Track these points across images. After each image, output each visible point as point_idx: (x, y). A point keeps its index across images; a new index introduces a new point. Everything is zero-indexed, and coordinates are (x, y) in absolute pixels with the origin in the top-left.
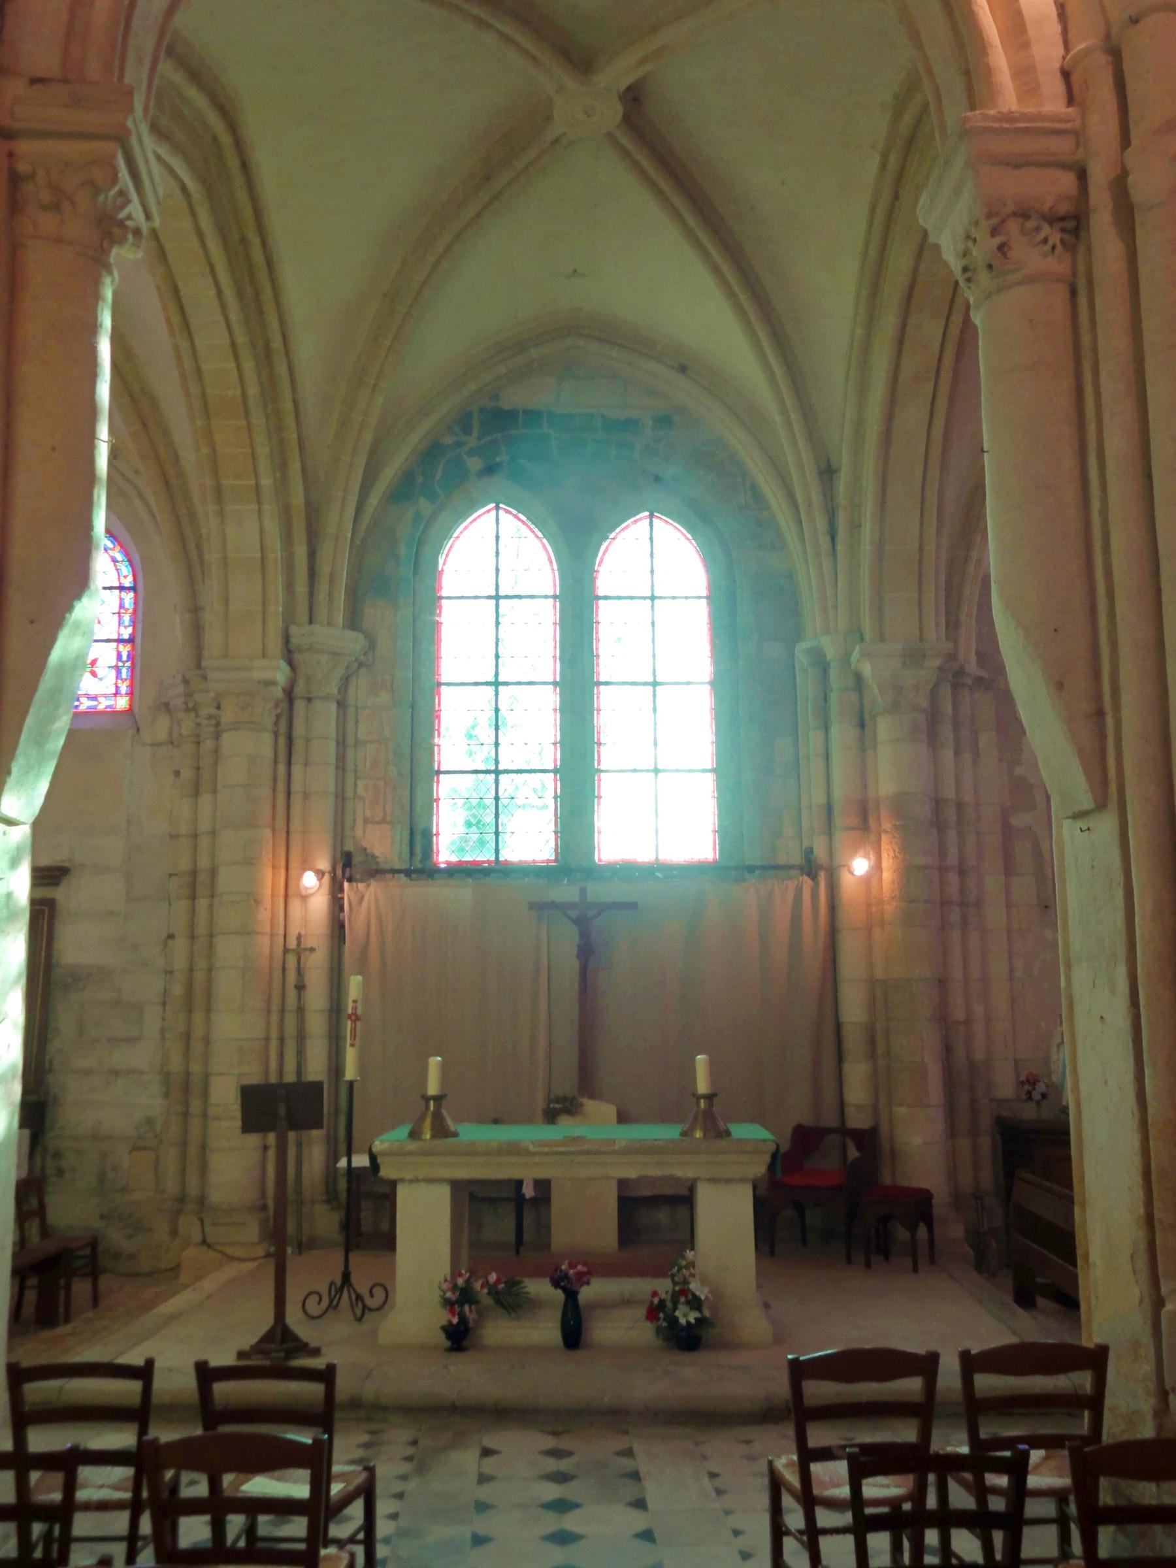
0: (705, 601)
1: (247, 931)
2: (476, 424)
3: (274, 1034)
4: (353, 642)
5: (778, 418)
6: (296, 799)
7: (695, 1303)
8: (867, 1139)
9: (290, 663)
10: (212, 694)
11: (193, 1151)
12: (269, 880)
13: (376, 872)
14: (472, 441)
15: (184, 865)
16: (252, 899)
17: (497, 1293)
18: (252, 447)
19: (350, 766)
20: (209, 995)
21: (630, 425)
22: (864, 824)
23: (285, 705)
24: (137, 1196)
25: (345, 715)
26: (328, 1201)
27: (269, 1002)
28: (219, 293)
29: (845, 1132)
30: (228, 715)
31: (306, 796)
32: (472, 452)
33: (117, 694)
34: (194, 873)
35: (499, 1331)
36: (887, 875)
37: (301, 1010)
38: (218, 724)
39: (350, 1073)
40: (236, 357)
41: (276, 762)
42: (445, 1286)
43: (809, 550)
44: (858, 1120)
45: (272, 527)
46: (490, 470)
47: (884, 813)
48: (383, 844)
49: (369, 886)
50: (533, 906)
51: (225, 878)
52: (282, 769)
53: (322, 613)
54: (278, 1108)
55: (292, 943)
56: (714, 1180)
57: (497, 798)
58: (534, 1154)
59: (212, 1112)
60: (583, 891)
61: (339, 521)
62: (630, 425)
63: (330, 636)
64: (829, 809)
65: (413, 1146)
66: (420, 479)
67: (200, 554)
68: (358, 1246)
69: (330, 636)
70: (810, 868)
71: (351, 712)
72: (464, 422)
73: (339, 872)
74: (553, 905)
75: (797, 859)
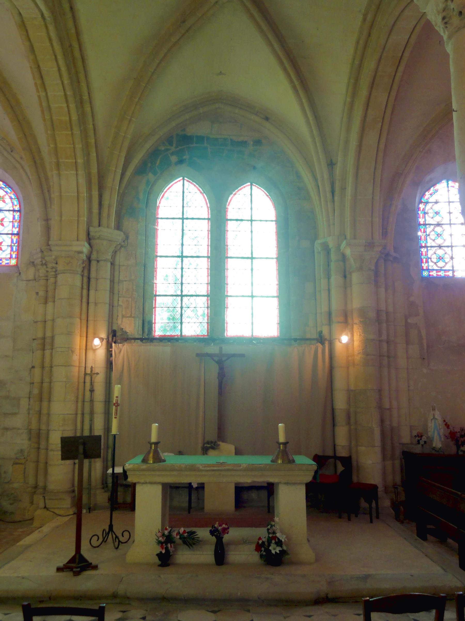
0: (274, 222)
1: (68, 365)
3: (80, 412)
4: (118, 236)
5: (310, 140)
6: (92, 306)
7: (279, 543)
8: (347, 461)
9: (90, 244)
10: (54, 257)
11: (41, 465)
12: (78, 342)
13: (126, 339)
14: (173, 149)
15: (40, 335)
16: (70, 350)
17: (185, 538)
18: (74, 143)
19: (116, 291)
20: (50, 393)
21: (244, 143)
22: (346, 321)
23: (87, 263)
24: (15, 485)
25: (114, 269)
26: (103, 488)
27: (77, 397)
28: (59, 70)
29: (335, 457)
30: (60, 267)
31: (96, 304)
32: (172, 154)
33: (11, 258)
34: (44, 338)
35: (184, 556)
36: (357, 343)
37: (92, 401)
38: (56, 271)
39: (114, 431)
40: (67, 101)
41: (82, 288)
42: (159, 534)
43: (322, 200)
44: (342, 453)
45: (82, 181)
46: (181, 162)
47: (355, 315)
48: (130, 326)
49: (123, 345)
50: (198, 355)
51: (59, 341)
52: (85, 292)
53: (104, 221)
54: (79, 448)
55: (88, 371)
56: (287, 484)
58: (202, 470)
59: (50, 447)
60: (221, 349)
61: (113, 181)
62: (244, 143)
63: (108, 232)
64: (330, 314)
65: (144, 466)
66: (149, 165)
67: (50, 194)
68: (116, 509)
69: (108, 232)
70: (321, 340)
71: (117, 267)
72: (169, 140)
73: (110, 339)
74: (208, 355)
75: (315, 336)
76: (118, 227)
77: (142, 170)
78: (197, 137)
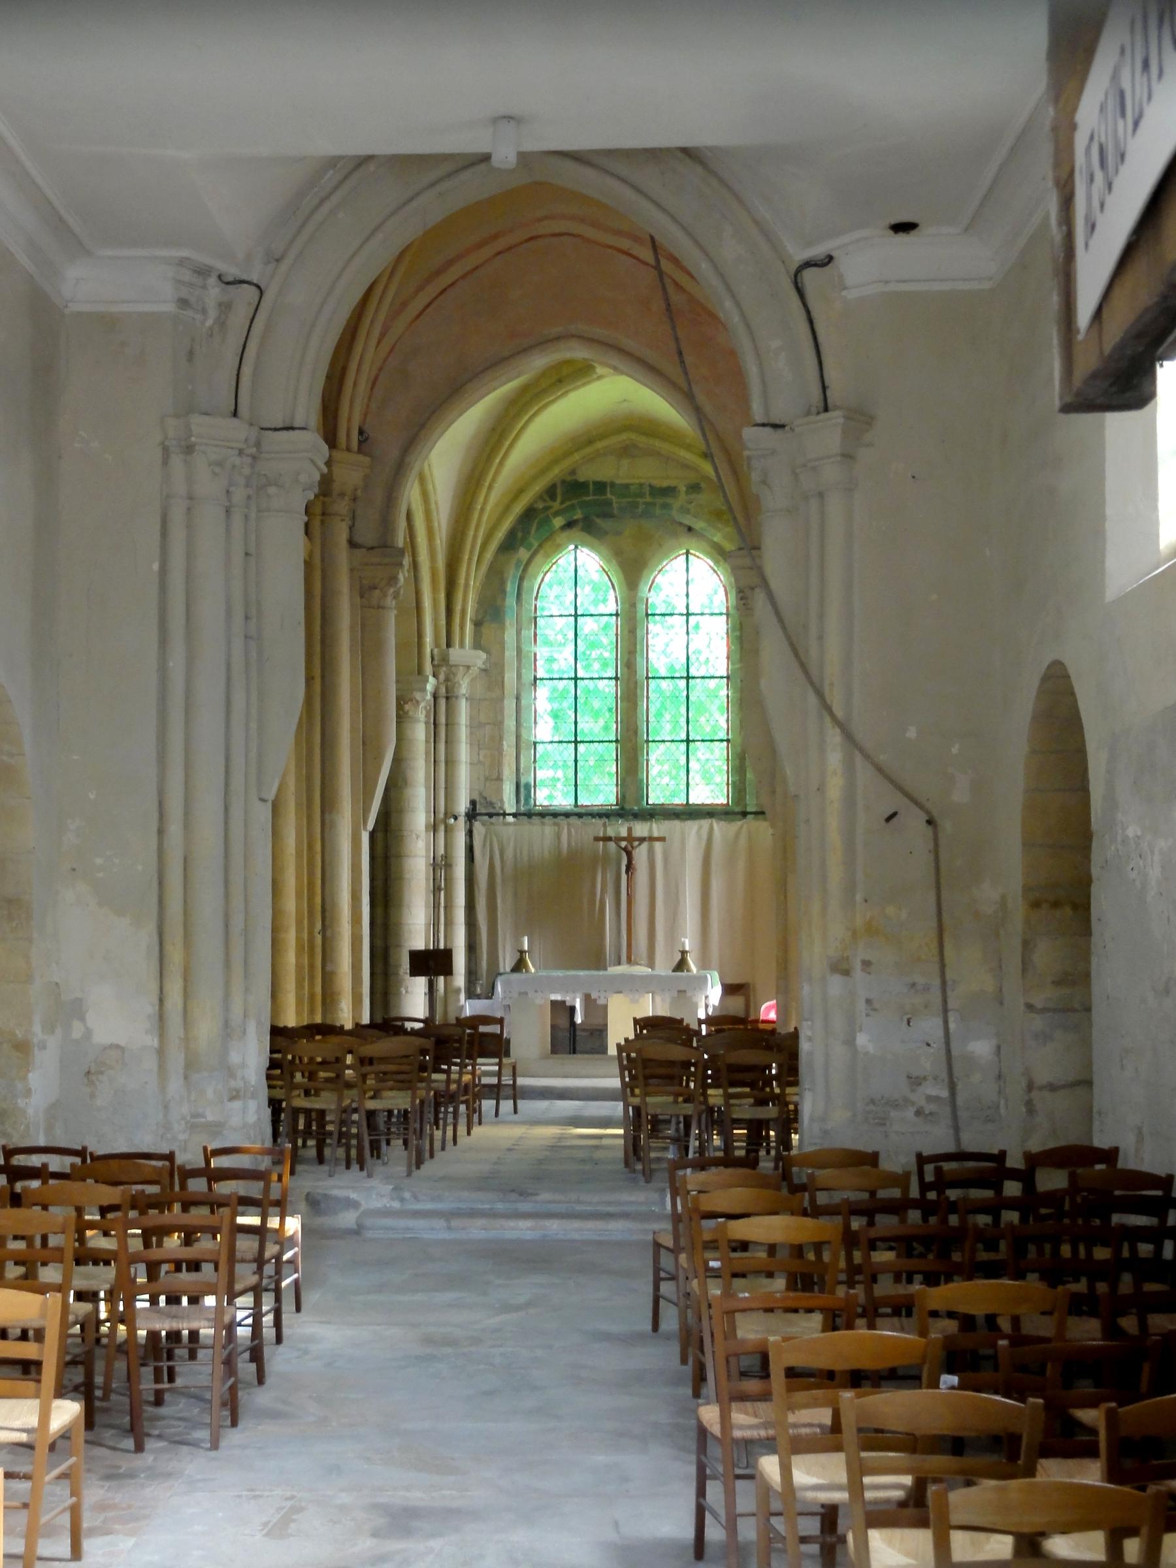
0: (725, 617)
2: (559, 491)
14: (556, 505)
32: (556, 514)
57: (576, 761)
66: (520, 535)
72: (551, 492)
76: (477, 645)
77: (510, 544)
78: (596, 483)
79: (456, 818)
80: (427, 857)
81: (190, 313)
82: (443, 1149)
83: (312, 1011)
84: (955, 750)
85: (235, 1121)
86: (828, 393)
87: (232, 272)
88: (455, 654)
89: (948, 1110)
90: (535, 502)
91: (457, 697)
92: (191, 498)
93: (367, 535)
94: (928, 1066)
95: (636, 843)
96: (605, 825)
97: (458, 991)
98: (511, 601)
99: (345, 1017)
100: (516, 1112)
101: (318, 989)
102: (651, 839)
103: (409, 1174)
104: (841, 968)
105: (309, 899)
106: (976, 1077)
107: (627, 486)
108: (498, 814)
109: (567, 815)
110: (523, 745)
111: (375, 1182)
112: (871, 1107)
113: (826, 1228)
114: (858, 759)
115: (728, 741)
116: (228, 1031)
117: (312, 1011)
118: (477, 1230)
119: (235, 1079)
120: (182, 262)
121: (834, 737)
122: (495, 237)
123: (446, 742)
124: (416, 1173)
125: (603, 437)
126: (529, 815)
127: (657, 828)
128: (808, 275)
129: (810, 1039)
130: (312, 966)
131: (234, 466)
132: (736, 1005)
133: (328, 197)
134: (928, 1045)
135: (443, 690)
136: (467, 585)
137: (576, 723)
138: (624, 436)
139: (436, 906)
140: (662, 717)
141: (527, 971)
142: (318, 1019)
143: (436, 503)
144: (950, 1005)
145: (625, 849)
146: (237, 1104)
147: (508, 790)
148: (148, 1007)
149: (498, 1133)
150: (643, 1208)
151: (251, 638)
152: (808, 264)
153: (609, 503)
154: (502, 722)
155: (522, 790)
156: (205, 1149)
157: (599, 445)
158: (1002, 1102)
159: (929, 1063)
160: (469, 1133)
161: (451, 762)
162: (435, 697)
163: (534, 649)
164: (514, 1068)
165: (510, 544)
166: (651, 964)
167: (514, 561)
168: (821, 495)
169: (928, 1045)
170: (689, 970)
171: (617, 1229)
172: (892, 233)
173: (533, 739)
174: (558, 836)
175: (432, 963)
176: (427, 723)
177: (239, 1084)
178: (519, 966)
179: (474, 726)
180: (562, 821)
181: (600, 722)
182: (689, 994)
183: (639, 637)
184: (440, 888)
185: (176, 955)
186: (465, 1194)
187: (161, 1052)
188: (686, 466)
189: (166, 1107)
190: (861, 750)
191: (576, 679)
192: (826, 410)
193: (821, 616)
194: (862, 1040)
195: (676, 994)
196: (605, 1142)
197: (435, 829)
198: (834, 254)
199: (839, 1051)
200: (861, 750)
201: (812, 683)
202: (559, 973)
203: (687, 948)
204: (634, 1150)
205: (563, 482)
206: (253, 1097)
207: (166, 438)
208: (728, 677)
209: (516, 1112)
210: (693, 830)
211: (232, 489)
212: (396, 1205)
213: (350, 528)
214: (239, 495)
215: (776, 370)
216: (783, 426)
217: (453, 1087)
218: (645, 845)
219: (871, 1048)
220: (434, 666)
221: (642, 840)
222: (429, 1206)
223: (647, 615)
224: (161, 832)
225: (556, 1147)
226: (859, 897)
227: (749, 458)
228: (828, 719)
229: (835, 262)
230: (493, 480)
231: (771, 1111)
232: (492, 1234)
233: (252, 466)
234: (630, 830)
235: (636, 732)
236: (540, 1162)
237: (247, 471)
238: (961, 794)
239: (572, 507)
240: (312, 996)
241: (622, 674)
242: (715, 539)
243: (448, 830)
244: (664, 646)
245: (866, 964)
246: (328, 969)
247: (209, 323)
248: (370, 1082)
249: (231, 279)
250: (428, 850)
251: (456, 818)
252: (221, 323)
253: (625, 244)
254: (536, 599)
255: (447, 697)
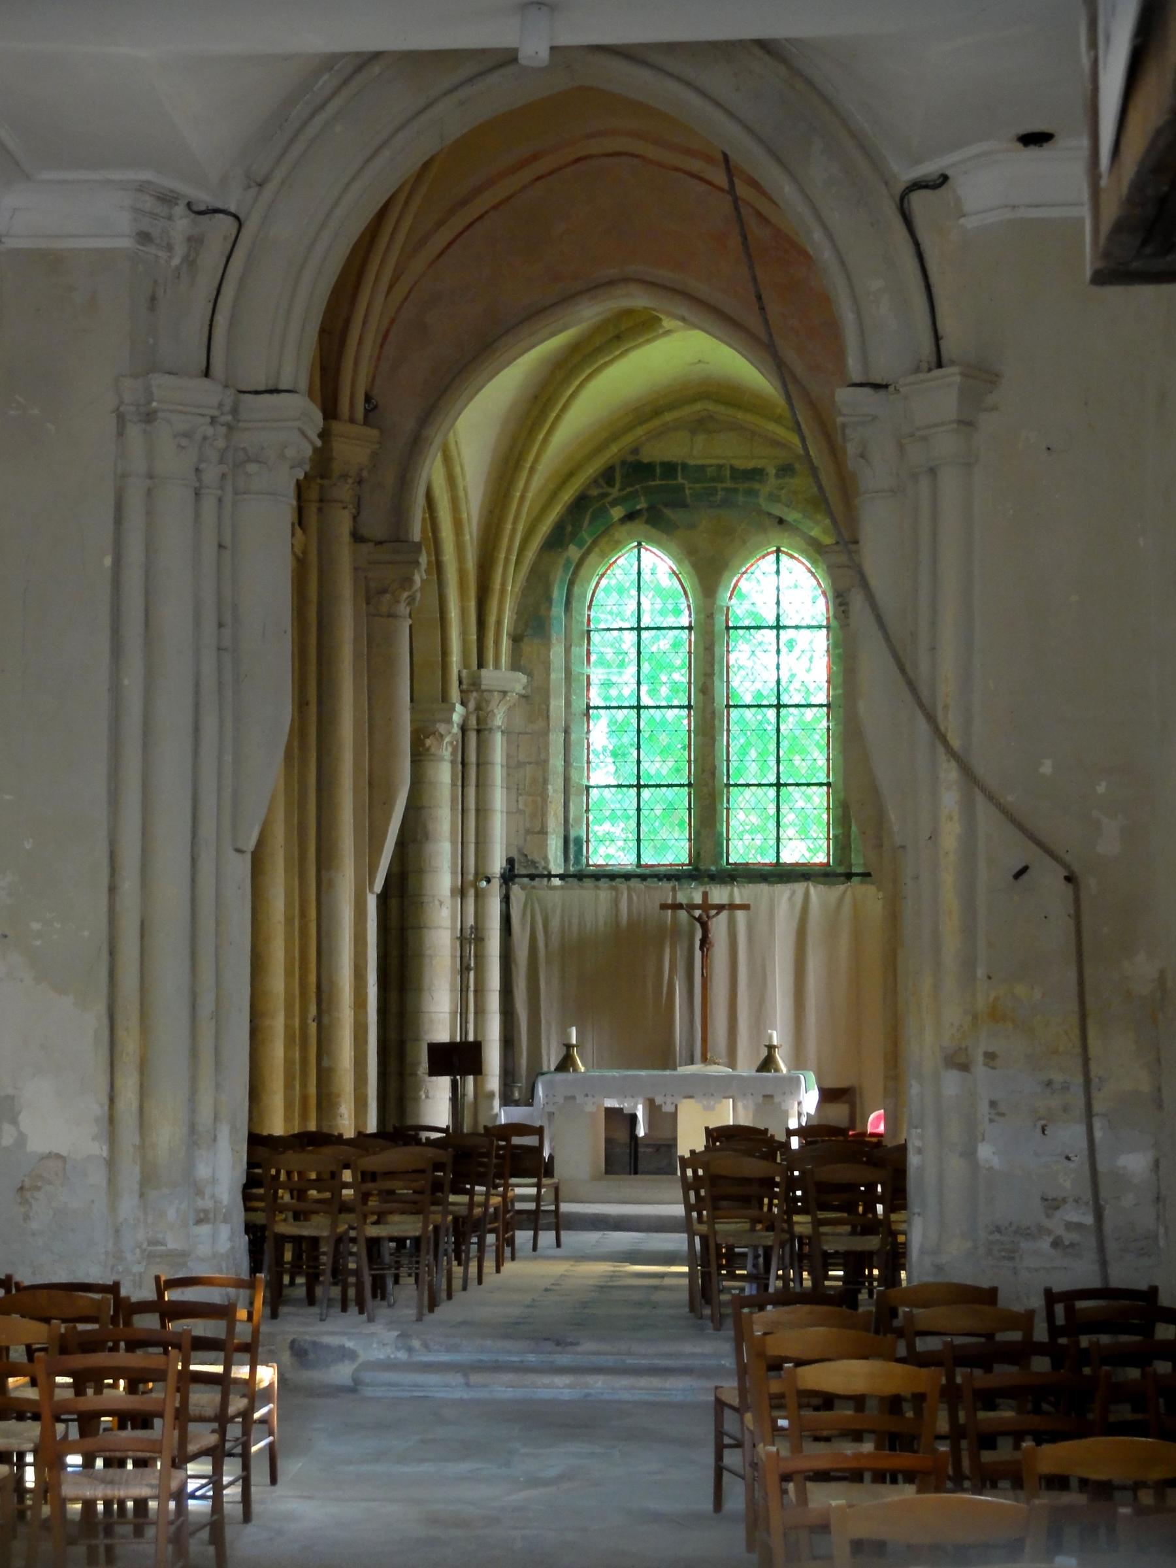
0: (824, 631)
14: (615, 492)
32: (614, 503)
57: (639, 810)
66: (569, 529)
72: (608, 475)
76: (515, 666)
79: (489, 881)
80: (453, 928)
81: (152, 249)
82: (465, 1288)
83: (304, 1116)
84: (1101, 789)
85: (203, 1250)
86: (943, 343)
87: (205, 198)
88: (489, 676)
89: (1091, 1242)
90: (588, 487)
91: (490, 730)
92: (150, 476)
93: (376, 524)
94: (1068, 1184)
95: (713, 912)
96: (674, 889)
97: (491, 1095)
98: (557, 610)
99: (346, 1125)
100: (558, 1245)
101: (312, 1090)
102: (732, 907)
103: (420, 1319)
104: (958, 1061)
105: (301, 978)
106: (1129, 1200)
107: (702, 468)
108: (542, 876)
109: (627, 876)
110: (573, 790)
111: (377, 1328)
112: (997, 1236)
113: (926, 1379)
114: (979, 797)
115: (828, 785)
116: (194, 1137)
117: (304, 1116)
118: (503, 1388)
119: (203, 1198)
120: (142, 187)
121: (950, 773)
122: (535, 157)
123: (477, 786)
124: (429, 1317)
125: (671, 407)
126: (580, 876)
127: (739, 893)
128: (918, 200)
129: (920, 1151)
130: (304, 1061)
131: (205, 438)
132: (838, 1114)
133: (322, 106)
134: (1068, 1158)
135: (473, 722)
136: (503, 591)
137: (639, 762)
138: (698, 406)
139: (464, 990)
140: (746, 753)
141: (576, 1070)
142: (312, 1127)
143: (465, 490)
144: (1097, 1107)
145: (699, 919)
146: (205, 1229)
147: (554, 845)
148: (96, 1106)
149: (536, 1270)
150: (713, 1362)
151: (225, 650)
152: (918, 185)
153: (681, 488)
154: (546, 761)
155: (572, 845)
156: (157, 1278)
157: (668, 417)
158: (1162, 1231)
159: (1069, 1181)
160: (498, 1271)
161: (482, 811)
162: (464, 729)
163: (586, 670)
164: (557, 1190)
165: (557, 540)
166: (732, 1064)
167: (562, 562)
168: (932, 471)
169: (1068, 1158)
170: (777, 1070)
171: (677, 1388)
172: (1020, 145)
173: (585, 782)
174: (616, 902)
175: (458, 1059)
176: (453, 762)
177: (208, 1204)
178: (566, 1064)
179: (511, 766)
180: (622, 885)
181: (668, 761)
182: (776, 1100)
183: (717, 659)
184: (468, 965)
185: (130, 1045)
186: (489, 1343)
187: (111, 1163)
188: (776, 443)
189: (117, 1231)
190: (983, 790)
191: (639, 707)
192: (940, 365)
193: (933, 623)
194: (985, 1152)
195: (760, 1100)
196: (667, 1281)
197: (463, 894)
198: (949, 172)
199: (956, 1165)
200: (983, 790)
201: (921, 705)
202: (615, 1073)
203: (775, 1043)
204: (703, 1292)
205: (623, 463)
206: (225, 1221)
207: (121, 403)
208: (828, 706)
209: (558, 1245)
210: (785, 896)
211: (203, 466)
212: (402, 1356)
213: (355, 518)
214: (211, 474)
215: (877, 316)
216: (886, 386)
217: (478, 1211)
218: (724, 915)
219: (996, 1162)
220: (462, 691)
221: (720, 908)
222: (445, 1358)
223: (728, 628)
224: (112, 890)
225: (605, 1288)
226: (980, 973)
227: (844, 426)
228: (941, 750)
229: (951, 182)
230: (536, 461)
231: (873, 1243)
232: (520, 1393)
233: (227, 437)
234: (705, 895)
235: (713, 774)
236: (584, 1305)
237: (221, 443)
238: (1109, 844)
239: (634, 496)
240: (304, 1099)
241: (699, 701)
242: (813, 534)
243: (479, 896)
244: (749, 668)
245: (990, 1056)
246: (325, 1063)
247: (176, 261)
248: (373, 1205)
249: (203, 208)
250: (453, 920)
251: (489, 881)
252: (190, 262)
253: (696, 165)
254: (590, 608)
255: (477, 729)
